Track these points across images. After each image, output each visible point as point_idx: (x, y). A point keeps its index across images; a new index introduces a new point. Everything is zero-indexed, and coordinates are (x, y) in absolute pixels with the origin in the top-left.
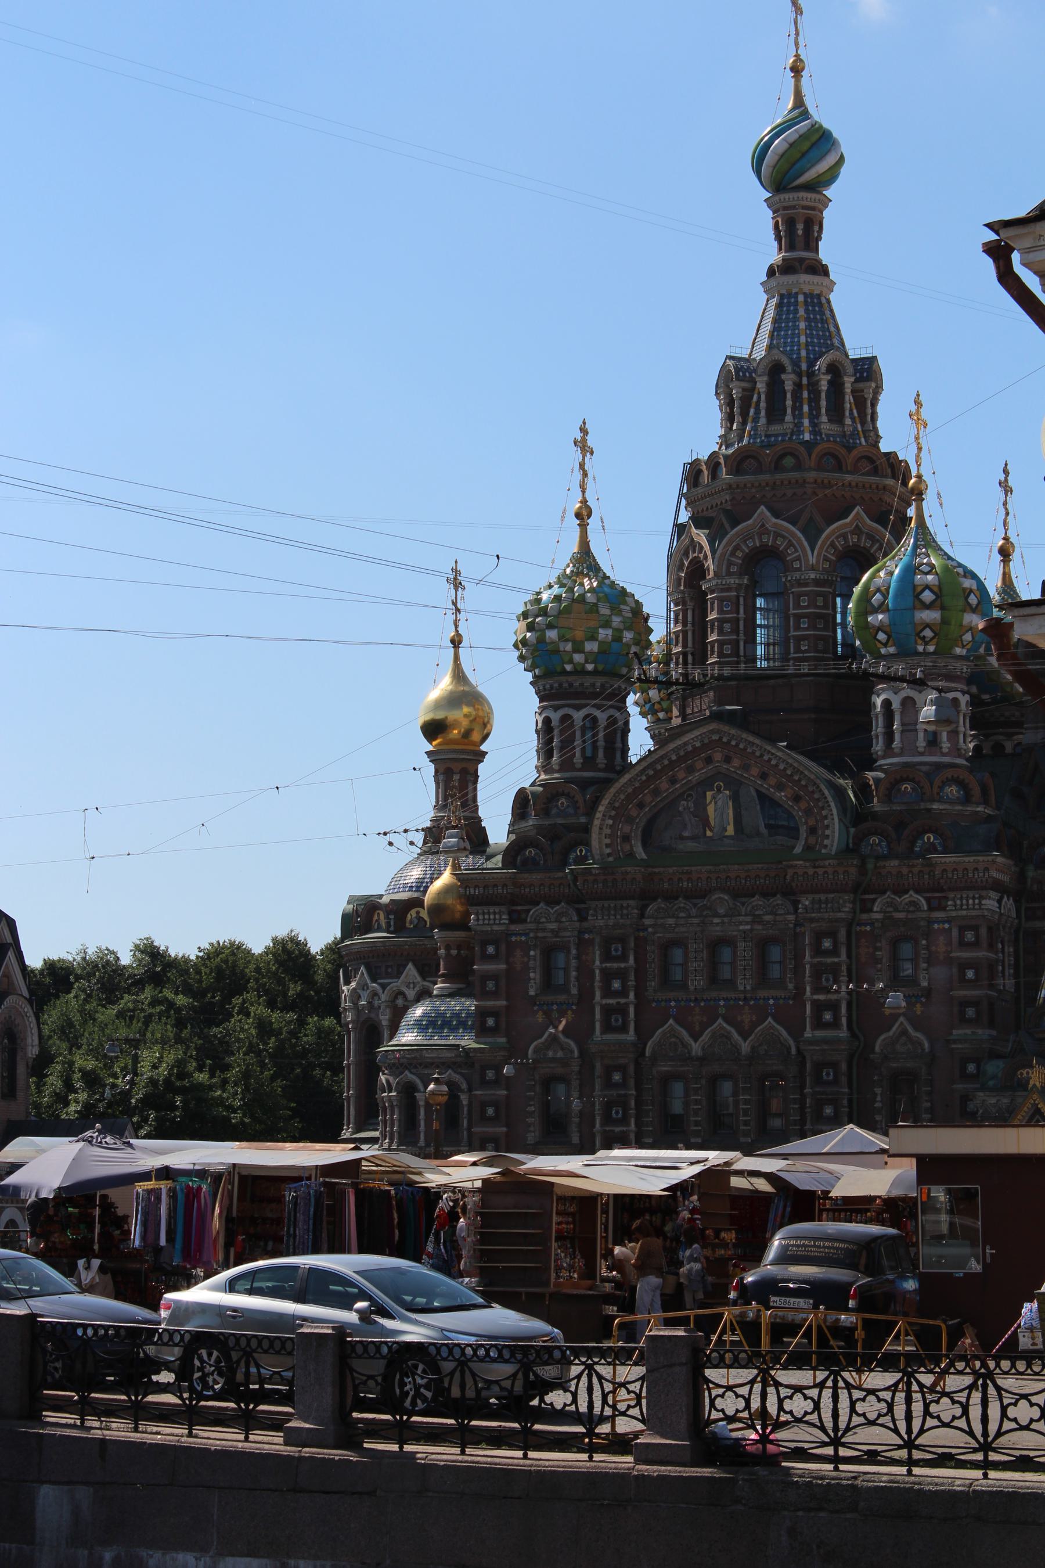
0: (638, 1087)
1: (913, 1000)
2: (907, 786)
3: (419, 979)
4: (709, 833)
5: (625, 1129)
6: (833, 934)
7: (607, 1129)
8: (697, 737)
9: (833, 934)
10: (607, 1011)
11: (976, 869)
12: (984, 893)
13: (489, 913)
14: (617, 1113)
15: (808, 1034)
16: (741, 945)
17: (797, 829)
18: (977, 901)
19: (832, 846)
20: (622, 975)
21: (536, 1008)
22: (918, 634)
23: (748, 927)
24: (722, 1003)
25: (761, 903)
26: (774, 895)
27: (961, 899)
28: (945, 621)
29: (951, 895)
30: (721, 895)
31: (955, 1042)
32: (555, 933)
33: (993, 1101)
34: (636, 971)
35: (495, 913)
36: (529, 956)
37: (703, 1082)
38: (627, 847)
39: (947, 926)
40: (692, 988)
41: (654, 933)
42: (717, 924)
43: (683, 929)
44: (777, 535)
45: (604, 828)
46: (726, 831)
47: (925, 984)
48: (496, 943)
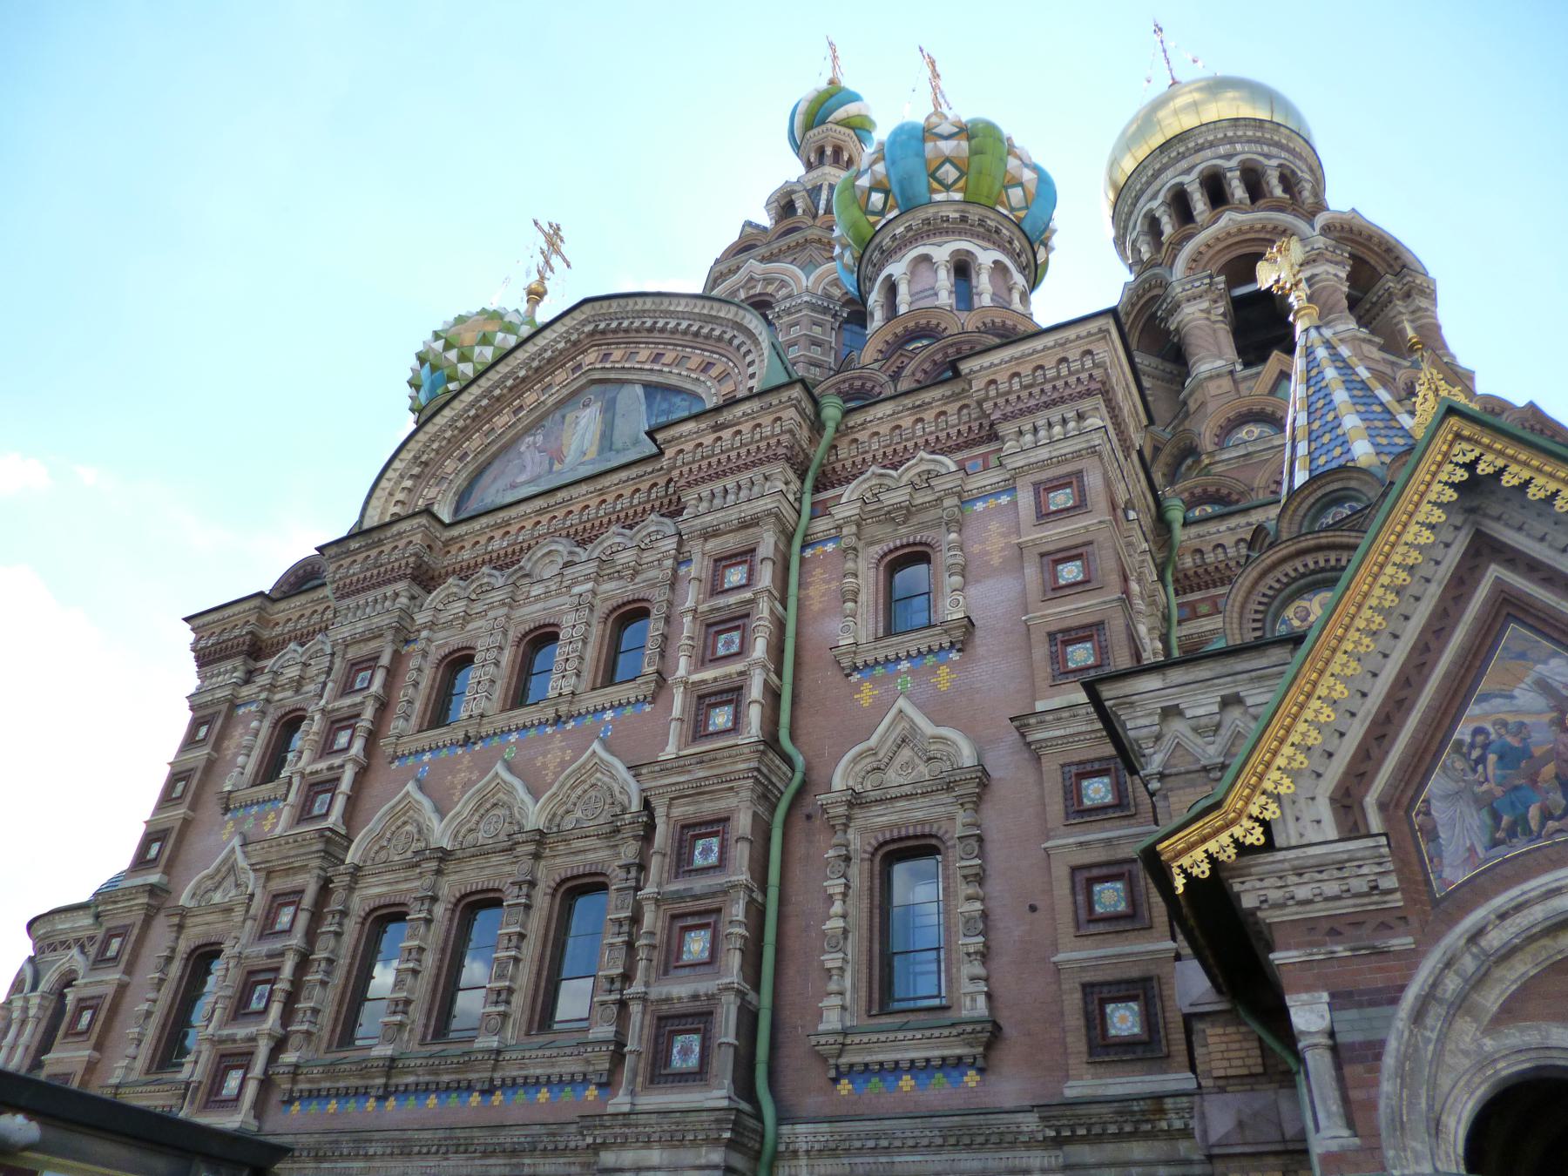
0: (311, 935)
1: (931, 659)
4: (557, 467)
6: (745, 556)
7: (225, 1032)
8: (561, 336)
9: (745, 556)
12: (1086, 405)
16: (568, 620)
18: (1072, 425)
21: (229, 815)
22: (932, 175)
23: (590, 585)
25: (618, 539)
28: (975, 152)
29: (1008, 429)
32: (298, 685)
33: (1203, 705)
34: (384, 706)
37: (440, 910)
39: (1004, 499)
41: (429, 640)
42: (538, 598)
44: (768, 281)
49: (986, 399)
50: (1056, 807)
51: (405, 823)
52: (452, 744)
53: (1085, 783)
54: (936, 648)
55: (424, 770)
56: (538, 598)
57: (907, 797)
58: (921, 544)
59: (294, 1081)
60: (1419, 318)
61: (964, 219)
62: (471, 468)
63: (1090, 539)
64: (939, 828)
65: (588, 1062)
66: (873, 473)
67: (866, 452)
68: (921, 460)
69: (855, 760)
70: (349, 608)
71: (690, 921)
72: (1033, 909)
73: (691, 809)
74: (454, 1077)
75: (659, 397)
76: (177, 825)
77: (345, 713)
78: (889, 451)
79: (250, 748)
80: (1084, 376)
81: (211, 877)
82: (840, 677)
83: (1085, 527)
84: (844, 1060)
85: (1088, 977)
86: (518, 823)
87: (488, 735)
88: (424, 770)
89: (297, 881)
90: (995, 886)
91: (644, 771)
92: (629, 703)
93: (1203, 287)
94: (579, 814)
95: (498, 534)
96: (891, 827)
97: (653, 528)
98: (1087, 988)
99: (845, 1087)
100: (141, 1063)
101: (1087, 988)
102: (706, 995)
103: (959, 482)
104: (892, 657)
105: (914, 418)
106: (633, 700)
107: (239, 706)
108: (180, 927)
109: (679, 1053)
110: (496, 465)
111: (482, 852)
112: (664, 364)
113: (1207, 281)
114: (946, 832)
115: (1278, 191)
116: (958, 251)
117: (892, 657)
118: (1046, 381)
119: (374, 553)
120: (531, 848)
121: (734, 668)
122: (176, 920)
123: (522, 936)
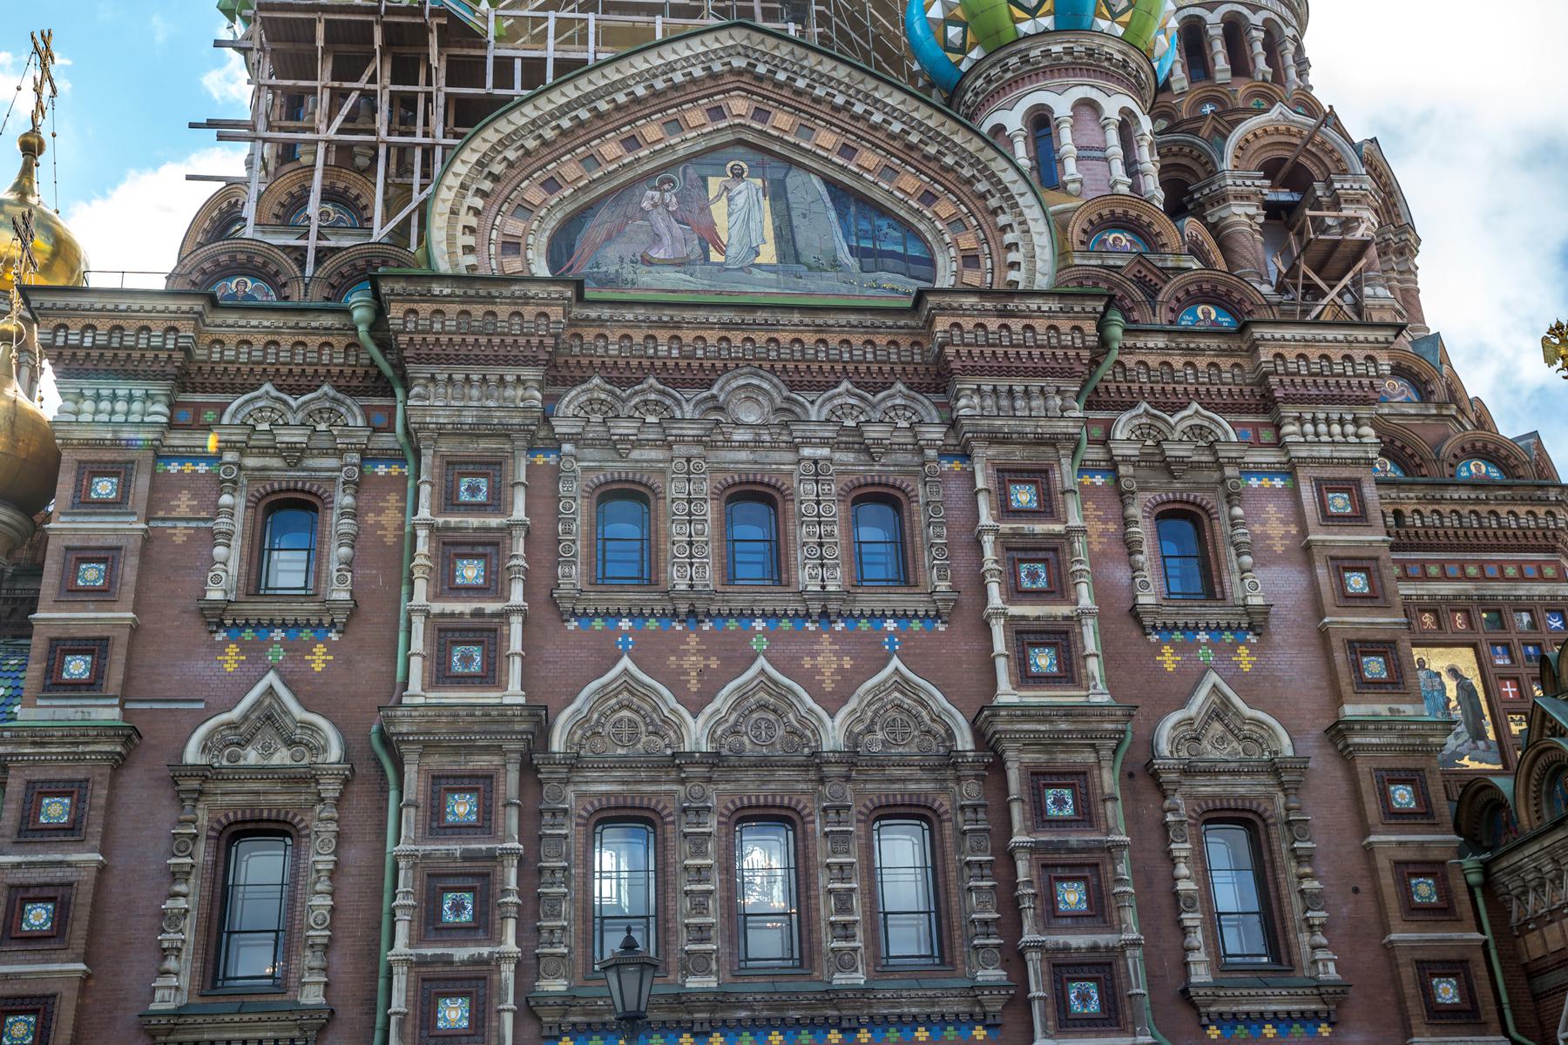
1: (1228, 637)
2: (1124, 239)
4: (715, 256)
5: (485, 951)
6: (1038, 476)
7: (429, 952)
8: (696, 56)
9: (1038, 476)
10: (447, 634)
11: (1347, 357)
12: (1364, 412)
13: (114, 398)
14: (458, 908)
15: (1007, 693)
16: (807, 490)
17: (932, 263)
19: (1031, 280)
20: (488, 547)
21: (220, 636)
23: (826, 452)
24: (759, 625)
26: (887, 386)
27: (1314, 421)
29: (1290, 411)
30: (755, 381)
31: (1364, 725)
32: (296, 456)
35: (130, 399)
36: (217, 511)
37: (712, 824)
38: (513, 265)
39: (1278, 483)
40: (682, 586)
42: (743, 445)
45: (463, 211)
46: (758, 254)
47: (1256, 600)
48: (121, 471)
49: (1276, 373)
50: (1372, 808)
51: (622, 707)
52: (664, 614)
53: (1392, 788)
54: (1234, 625)
55: (625, 643)
56: (743, 445)
57: (1232, 773)
58: (1194, 504)
59: (564, 1016)
60: (1407, 281)
61: (1125, 65)
62: (569, 208)
63: (1375, 555)
64: (1259, 805)
65: (980, 1003)
66: (1145, 410)
67: (1134, 381)
68: (1197, 412)
69: (1174, 728)
70: (433, 379)
71: (1060, 872)
72: (1356, 890)
73: (1043, 757)
74: (803, 1012)
75: (853, 209)
76: (123, 637)
77: (471, 536)
78: (1158, 387)
79: (229, 535)
80: (1365, 381)
81: (232, 726)
82: (1136, 633)
83: (1370, 542)
84: (1213, 1009)
85: (1419, 955)
86: (801, 736)
87: (719, 614)
88: (625, 643)
89: (481, 762)
90: (1323, 869)
91: (1003, 713)
92: (916, 616)
93: (1252, 188)
94: (880, 736)
95: (663, 336)
96: (1213, 797)
97: (898, 401)
98: (1421, 964)
99: (1214, 1033)
100: (184, 982)
101: (1421, 964)
102: (1107, 947)
103: (1242, 454)
104: (1191, 625)
105: (1183, 360)
106: (921, 613)
107: (169, 458)
108: (201, 793)
109: (1077, 998)
110: (604, 214)
111: (764, 764)
112: (859, 166)
113: (1257, 183)
114: (1266, 810)
115: (1292, 72)
116: (1125, 111)
117: (1191, 625)
118: (1333, 375)
119: (478, 310)
120: (843, 770)
121: (1063, 610)
122: (194, 784)
123: (852, 864)
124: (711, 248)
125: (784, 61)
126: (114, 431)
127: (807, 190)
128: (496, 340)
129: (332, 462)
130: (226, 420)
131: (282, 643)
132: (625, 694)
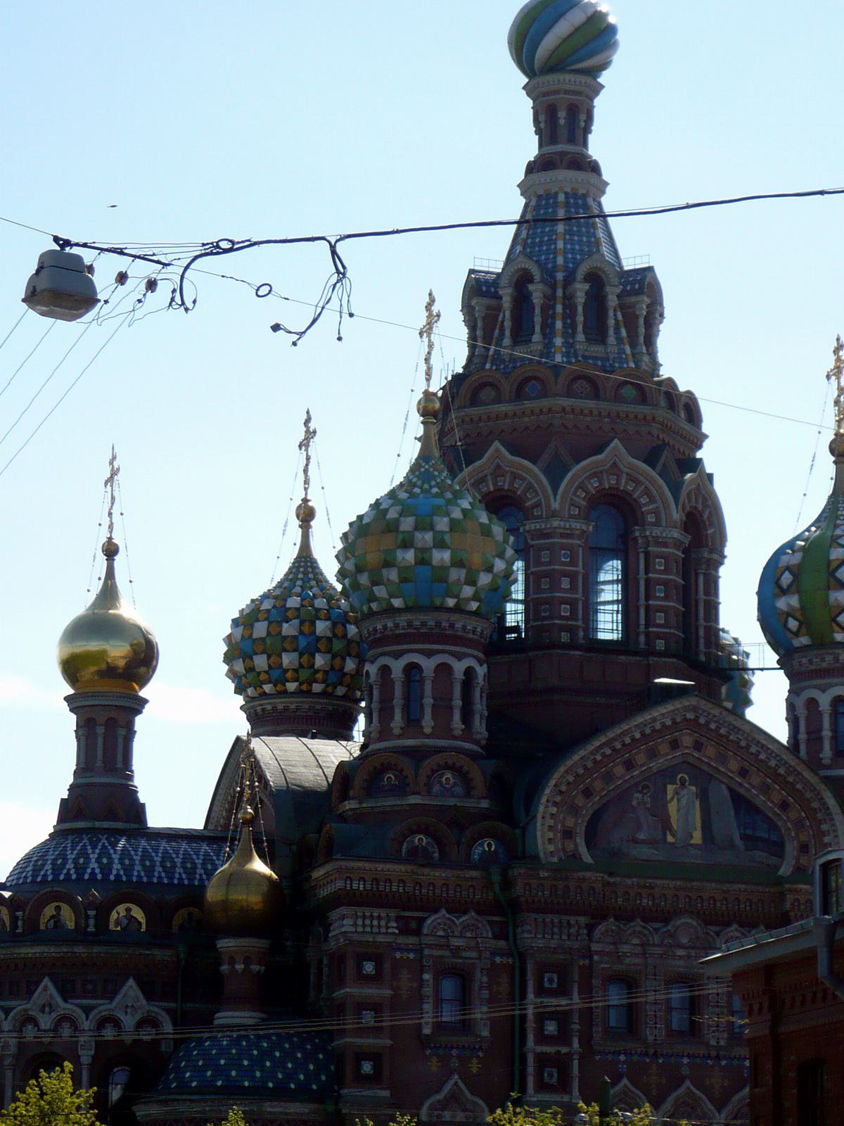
3: (144, 1002)
4: (670, 839)
10: (542, 1061)
13: (372, 917)
21: (428, 1052)
38: (570, 846)
42: (681, 957)
43: (637, 961)
48: (378, 959)
124: (668, 832)
125: (714, 716)
126: (374, 938)
127: (720, 793)
128: (568, 902)
129: (474, 954)
130: (425, 931)
131: (458, 1056)
132: (623, 1096)
